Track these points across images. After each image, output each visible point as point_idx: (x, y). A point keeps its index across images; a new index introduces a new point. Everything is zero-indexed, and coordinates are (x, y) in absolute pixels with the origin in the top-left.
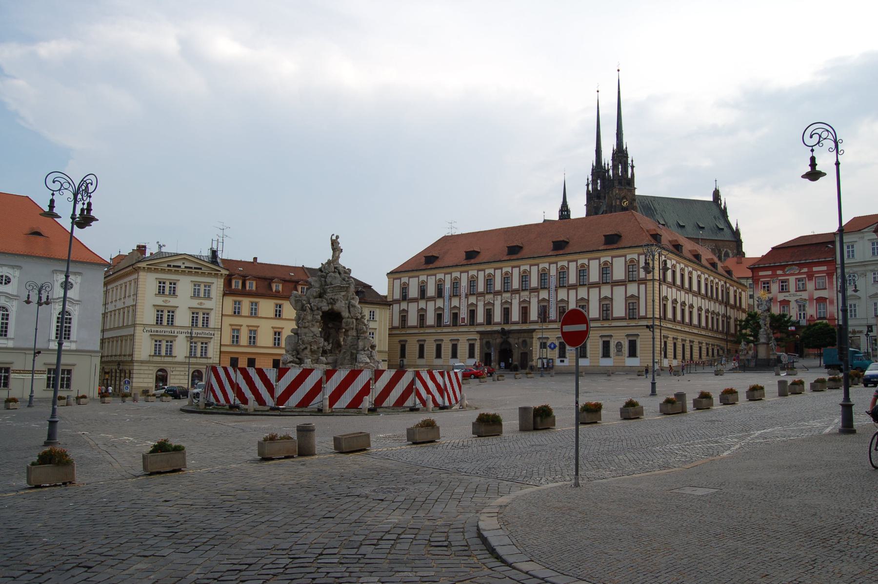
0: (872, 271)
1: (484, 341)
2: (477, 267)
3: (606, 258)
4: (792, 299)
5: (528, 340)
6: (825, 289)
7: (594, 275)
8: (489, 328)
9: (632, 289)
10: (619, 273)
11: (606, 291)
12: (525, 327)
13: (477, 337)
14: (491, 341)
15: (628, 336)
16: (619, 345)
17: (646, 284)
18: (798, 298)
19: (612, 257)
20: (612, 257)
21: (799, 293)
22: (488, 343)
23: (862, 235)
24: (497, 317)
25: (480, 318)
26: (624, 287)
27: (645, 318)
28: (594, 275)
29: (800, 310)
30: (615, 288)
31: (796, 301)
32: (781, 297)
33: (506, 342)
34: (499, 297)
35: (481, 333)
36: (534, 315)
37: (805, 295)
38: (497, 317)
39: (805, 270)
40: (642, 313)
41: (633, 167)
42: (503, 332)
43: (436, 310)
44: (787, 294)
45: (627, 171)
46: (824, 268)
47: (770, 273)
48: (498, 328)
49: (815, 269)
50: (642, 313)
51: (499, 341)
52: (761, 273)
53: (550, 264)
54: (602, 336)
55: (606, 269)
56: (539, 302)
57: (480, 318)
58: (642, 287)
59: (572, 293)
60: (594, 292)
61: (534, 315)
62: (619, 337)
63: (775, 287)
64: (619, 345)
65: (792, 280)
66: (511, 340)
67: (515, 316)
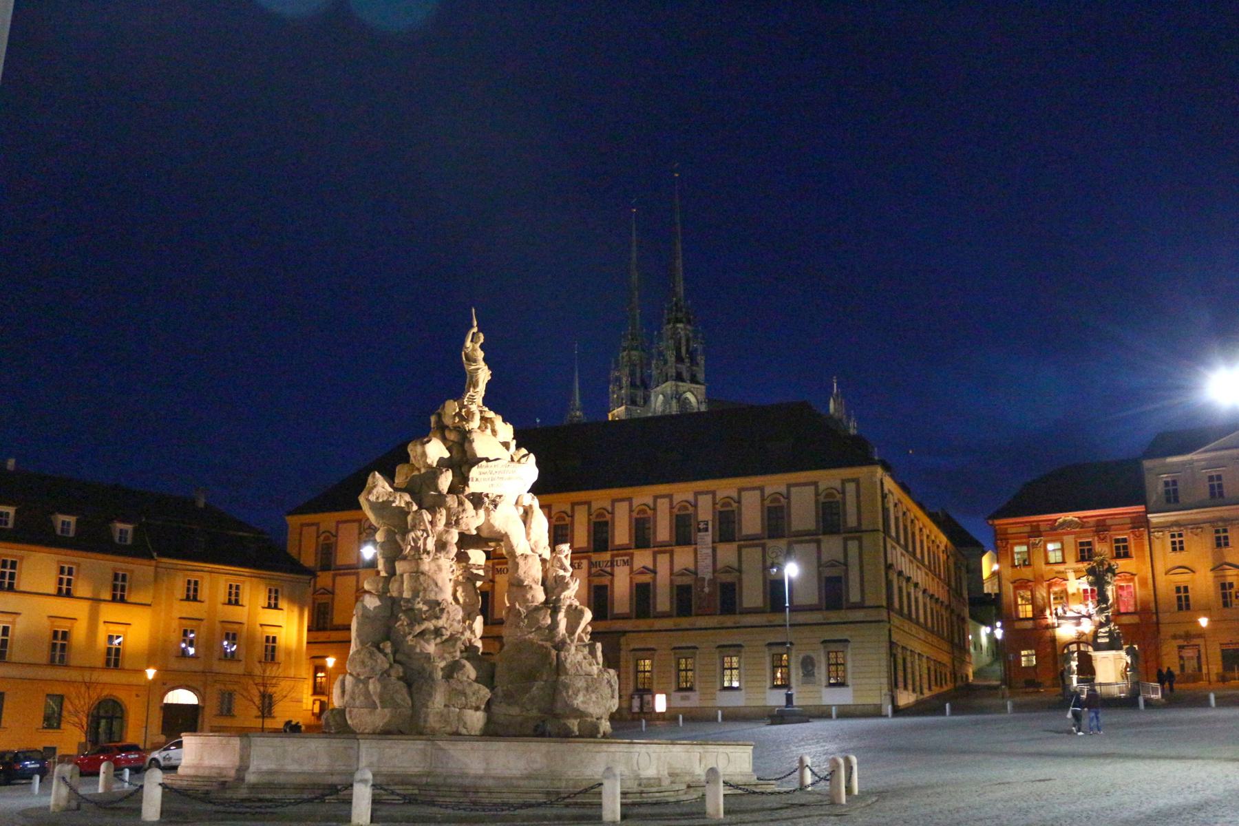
17: (860, 539)
27: (860, 606)
50: (855, 597)
58: (853, 546)
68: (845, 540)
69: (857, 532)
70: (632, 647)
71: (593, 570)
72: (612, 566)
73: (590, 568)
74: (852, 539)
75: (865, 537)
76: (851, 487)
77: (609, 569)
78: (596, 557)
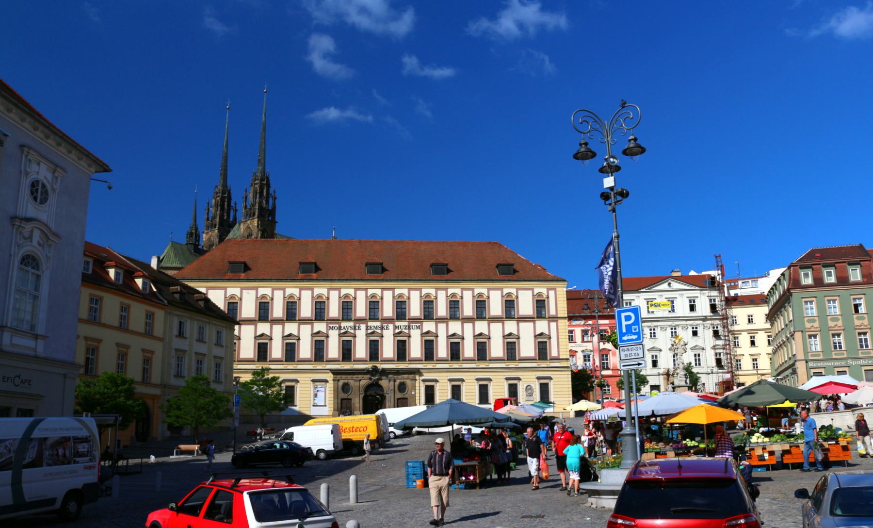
1: (341, 383)
2: (328, 284)
3: (510, 288)
5: (409, 383)
7: (496, 307)
8: (347, 366)
9: (542, 326)
10: (526, 306)
11: (511, 326)
12: (402, 366)
13: (329, 377)
14: (352, 382)
15: (539, 378)
16: (528, 388)
19: (518, 289)
20: (518, 289)
21: (584, 344)
22: (346, 388)
24: (361, 350)
25: (333, 350)
26: (531, 324)
28: (496, 307)
29: (585, 360)
30: (522, 324)
31: (583, 351)
33: (374, 386)
34: (363, 327)
35: (335, 372)
36: (416, 349)
38: (361, 350)
39: (590, 322)
40: (554, 353)
41: (275, 199)
42: (375, 370)
43: (256, 337)
45: (267, 202)
46: (607, 322)
48: (369, 366)
50: (554, 353)
51: (365, 381)
53: (437, 289)
54: (507, 379)
55: (510, 305)
56: (423, 335)
57: (333, 350)
59: (468, 326)
60: (496, 328)
61: (416, 349)
62: (529, 380)
64: (528, 388)
66: (384, 383)
67: (388, 350)
68: (549, 322)
69: (555, 319)
70: (422, 378)
71: (397, 331)
72: (409, 329)
73: (394, 330)
74: (553, 321)
75: (560, 321)
76: (552, 293)
77: (407, 331)
78: (398, 324)
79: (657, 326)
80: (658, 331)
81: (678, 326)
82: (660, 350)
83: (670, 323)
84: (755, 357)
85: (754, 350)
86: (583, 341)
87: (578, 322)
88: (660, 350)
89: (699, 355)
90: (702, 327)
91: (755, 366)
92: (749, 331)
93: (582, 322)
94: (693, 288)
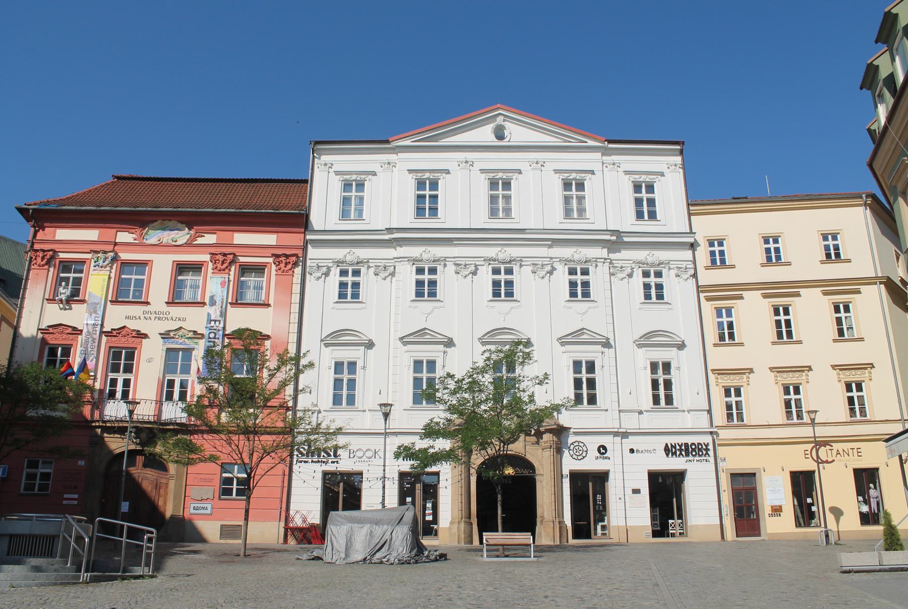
0: (414, 261)
4: (153, 328)
6: (269, 305)
18: (174, 326)
21: (176, 311)
23: (392, 157)
29: (169, 367)
31: (166, 336)
32: (117, 317)
37: (195, 319)
39: (210, 239)
44: (137, 310)
46: (269, 239)
47: (91, 234)
49: (241, 238)
52: (63, 234)
63: (97, 282)
65: (162, 268)
79: (444, 261)
80: (446, 278)
81: (520, 261)
82: (450, 343)
83: (491, 252)
84: (791, 379)
85: (788, 355)
86: (175, 299)
87: (167, 236)
88: (450, 343)
89: (591, 367)
90: (604, 269)
91: (792, 408)
92: (769, 289)
93: (182, 236)
94: (575, 139)
